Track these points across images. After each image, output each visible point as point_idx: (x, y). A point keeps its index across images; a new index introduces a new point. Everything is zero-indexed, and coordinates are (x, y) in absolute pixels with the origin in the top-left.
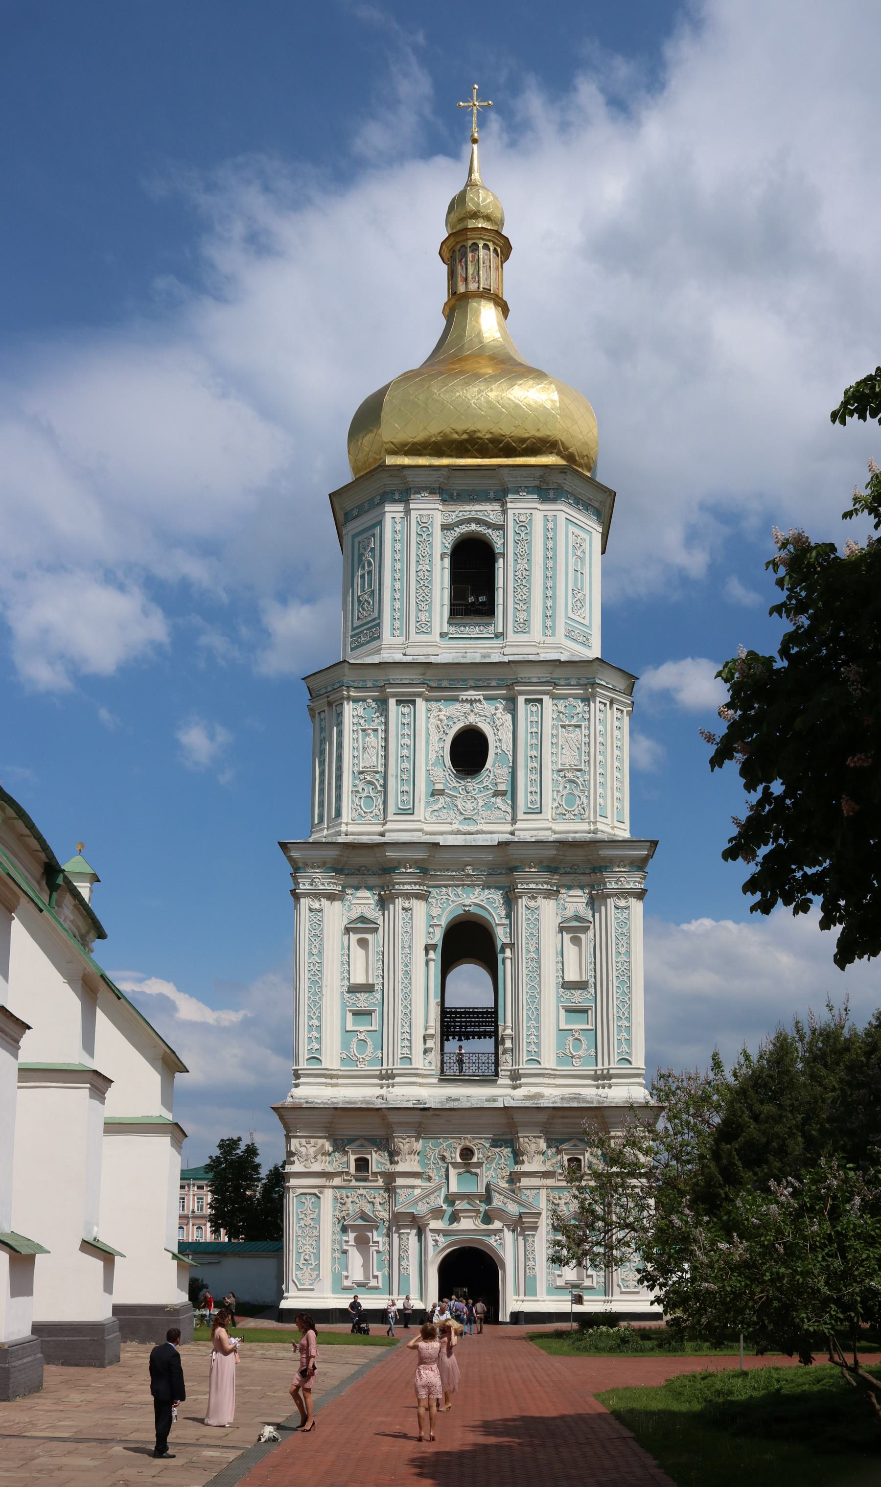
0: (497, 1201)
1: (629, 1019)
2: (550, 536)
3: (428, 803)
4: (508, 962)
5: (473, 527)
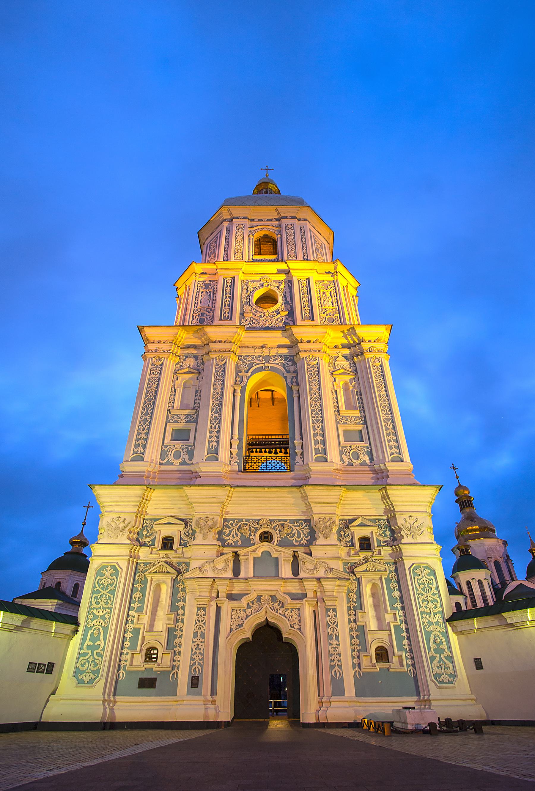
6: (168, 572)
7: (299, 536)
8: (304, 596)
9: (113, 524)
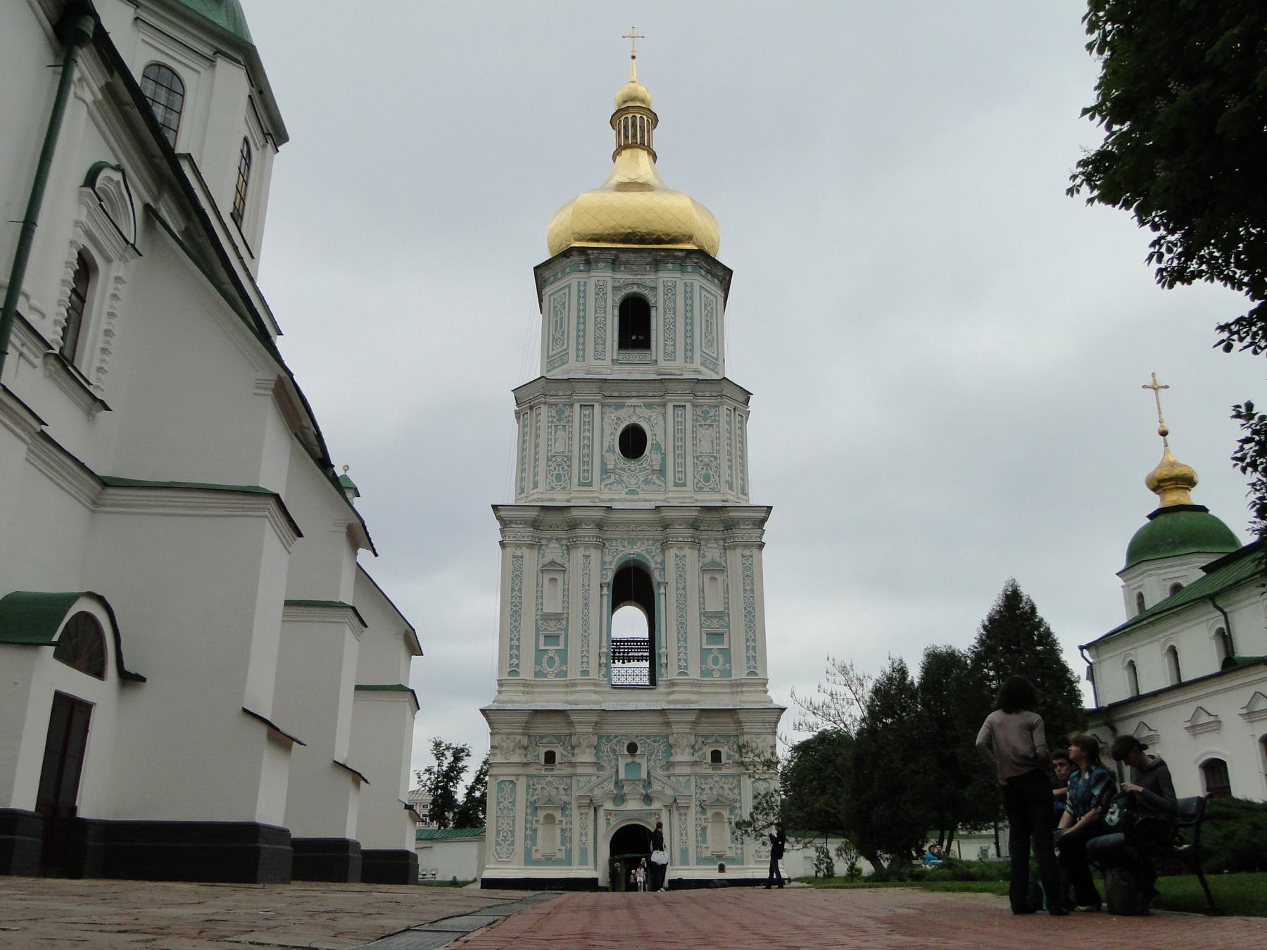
0: (656, 786)
1: (754, 641)
2: (689, 296)
3: (602, 480)
4: (662, 597)
5: (635, 289)
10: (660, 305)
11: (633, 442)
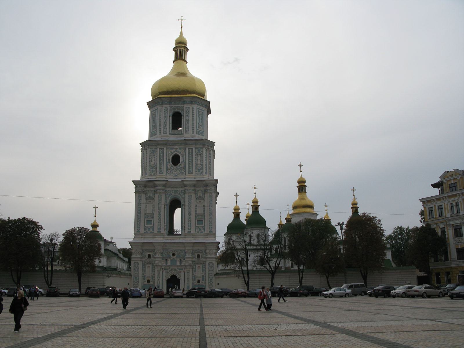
5: (177, 110)
6: (150, 264)
7: (182, 254)
8: (182, 269)
9: (136, 252)
10: (185, 116)
11: (176, 160)
